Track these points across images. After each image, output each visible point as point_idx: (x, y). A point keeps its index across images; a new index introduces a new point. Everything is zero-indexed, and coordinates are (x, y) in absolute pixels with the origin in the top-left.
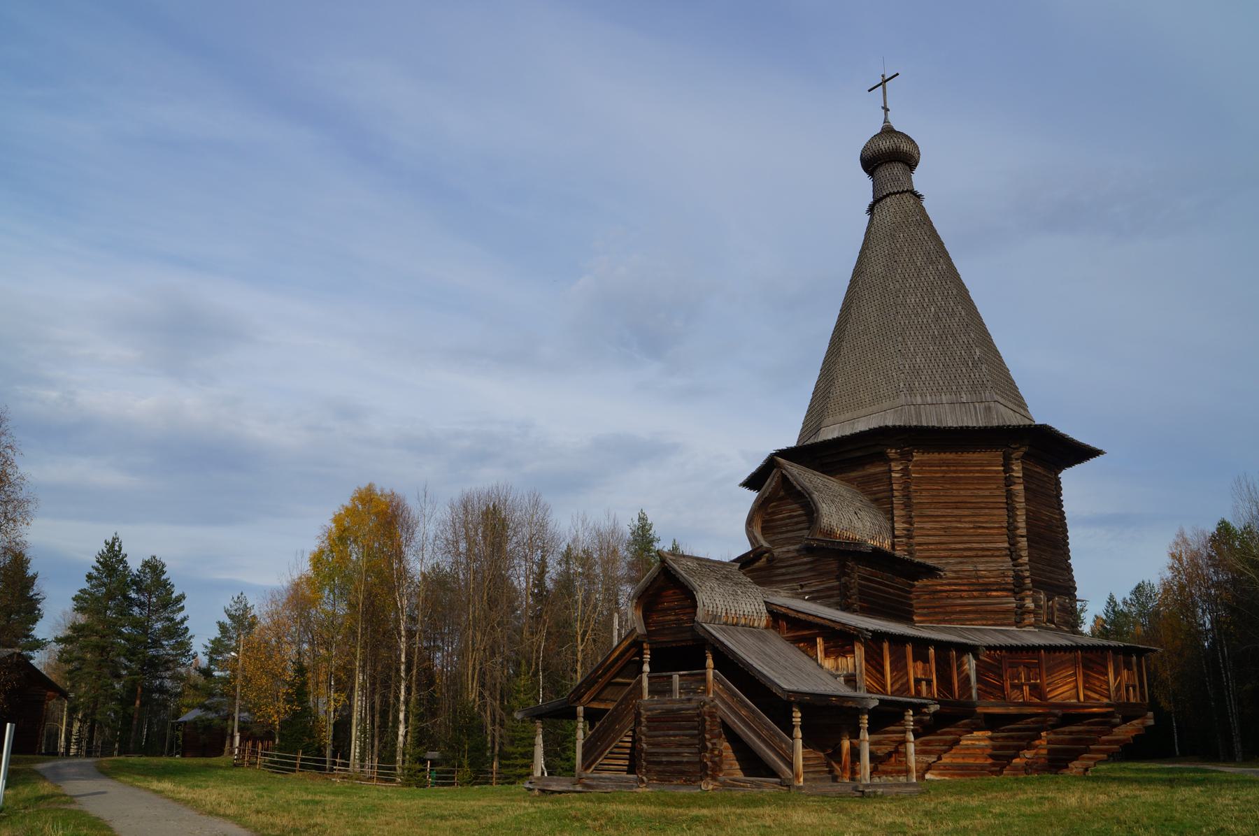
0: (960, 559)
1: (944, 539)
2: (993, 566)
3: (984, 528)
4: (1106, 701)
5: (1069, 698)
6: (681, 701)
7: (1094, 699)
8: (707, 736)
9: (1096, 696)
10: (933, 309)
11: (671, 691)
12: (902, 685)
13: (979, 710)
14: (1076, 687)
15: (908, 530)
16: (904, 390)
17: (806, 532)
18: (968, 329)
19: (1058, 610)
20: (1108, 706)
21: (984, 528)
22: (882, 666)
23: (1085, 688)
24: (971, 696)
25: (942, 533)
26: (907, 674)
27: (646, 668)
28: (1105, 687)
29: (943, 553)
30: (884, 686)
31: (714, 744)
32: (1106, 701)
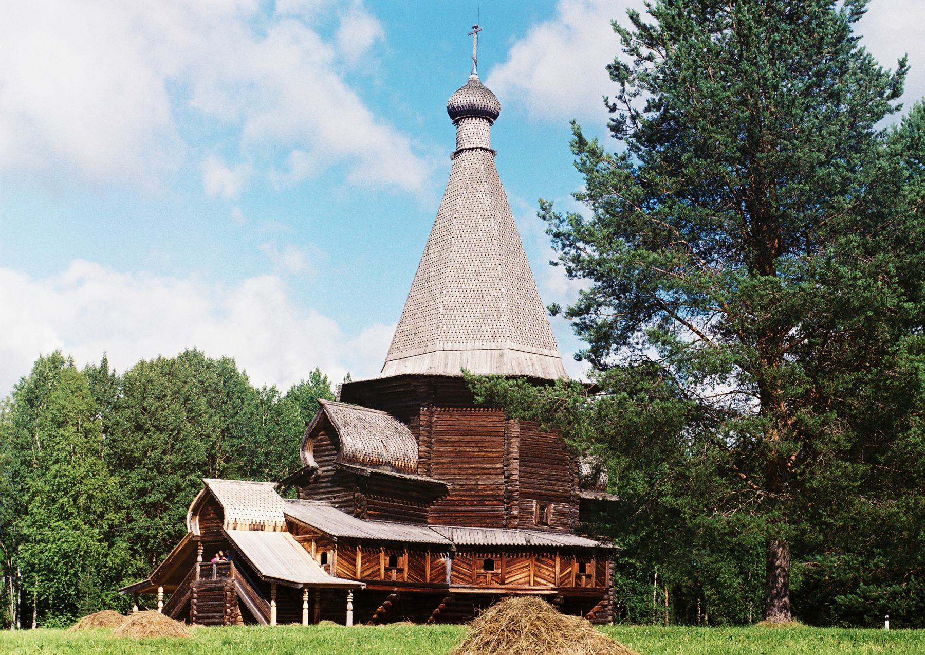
0: (465, 476)
1: (456, 460)
2: (491, 482)
3: (486, 452)
4: (552, 586)
5: (523, 584)
6: (216, 582)
7: (542, 584)
8: (228, 605)
9: (545, 582)
10: (476, 265)
11: (211, 575)
12: (373, 573)
13: (451, 590)
14: (530, 576)
15: (428, 453)
16: (440, 337)
17: (335, 457)
18: (500, 284)
19: (553, 514)
20: (553, 589)
21: (486, 452)
22: (355, 560)
23: (535, 576)
24: (445, 580)
25: (454, 455)
26: (378, 563)
27: (200, 559)
28: (552, 575)
29: (452, 471)
30: (355, 574)
31: (231, 610)
32: (552, 586)
